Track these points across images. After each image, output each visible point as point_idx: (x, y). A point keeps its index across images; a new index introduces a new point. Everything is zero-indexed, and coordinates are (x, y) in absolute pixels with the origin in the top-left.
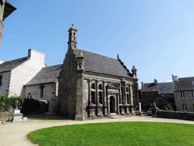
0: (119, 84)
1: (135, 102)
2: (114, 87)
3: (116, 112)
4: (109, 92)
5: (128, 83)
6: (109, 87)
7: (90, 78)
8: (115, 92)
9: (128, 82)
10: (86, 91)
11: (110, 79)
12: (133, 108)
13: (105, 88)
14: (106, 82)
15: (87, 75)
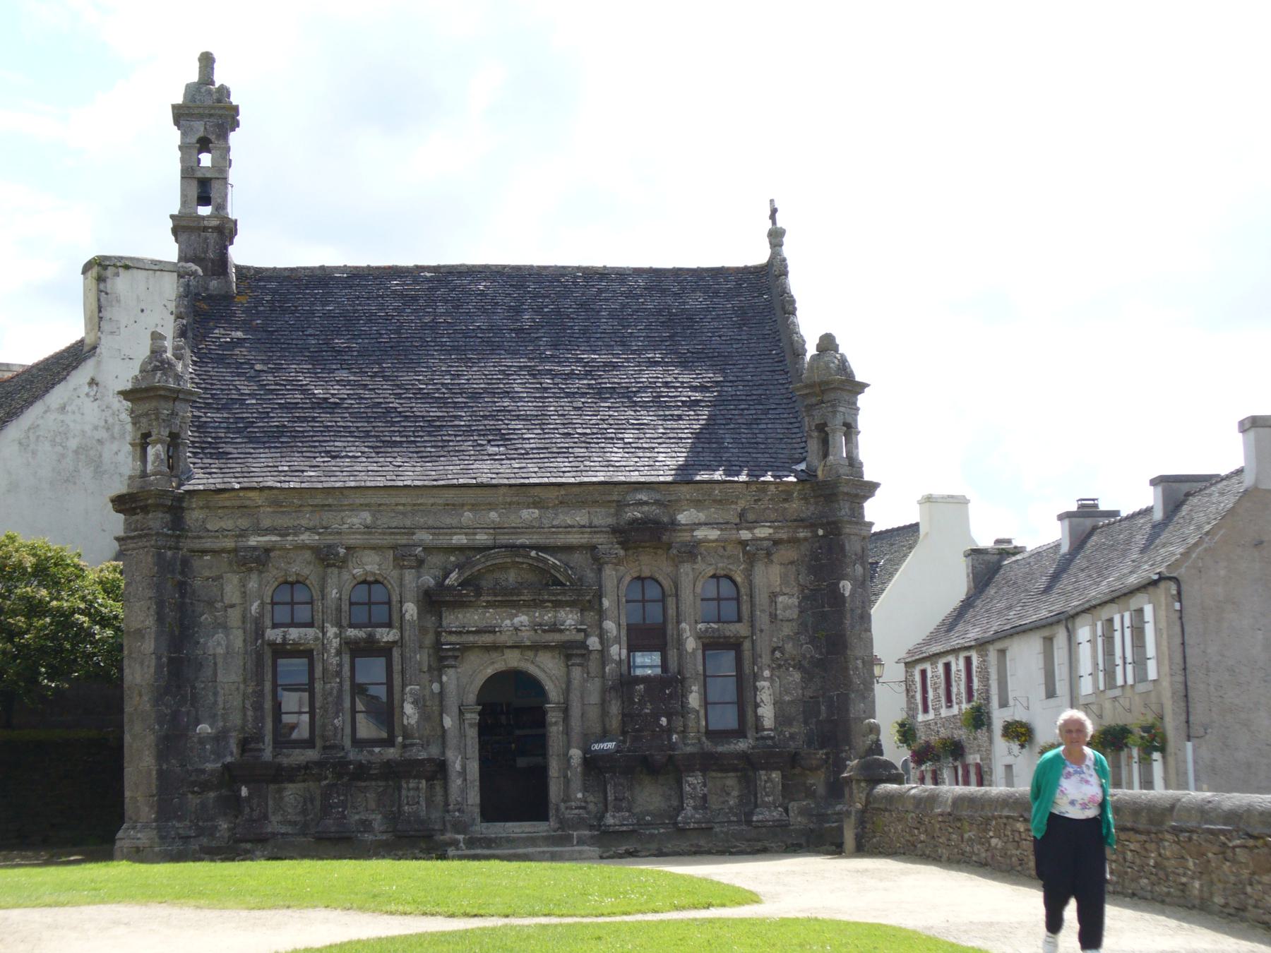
3: (552, 813)
4: (453, 639)
7: (253, 541)
8: (527, 637)
10: (220, 651)
12: (776, 776)
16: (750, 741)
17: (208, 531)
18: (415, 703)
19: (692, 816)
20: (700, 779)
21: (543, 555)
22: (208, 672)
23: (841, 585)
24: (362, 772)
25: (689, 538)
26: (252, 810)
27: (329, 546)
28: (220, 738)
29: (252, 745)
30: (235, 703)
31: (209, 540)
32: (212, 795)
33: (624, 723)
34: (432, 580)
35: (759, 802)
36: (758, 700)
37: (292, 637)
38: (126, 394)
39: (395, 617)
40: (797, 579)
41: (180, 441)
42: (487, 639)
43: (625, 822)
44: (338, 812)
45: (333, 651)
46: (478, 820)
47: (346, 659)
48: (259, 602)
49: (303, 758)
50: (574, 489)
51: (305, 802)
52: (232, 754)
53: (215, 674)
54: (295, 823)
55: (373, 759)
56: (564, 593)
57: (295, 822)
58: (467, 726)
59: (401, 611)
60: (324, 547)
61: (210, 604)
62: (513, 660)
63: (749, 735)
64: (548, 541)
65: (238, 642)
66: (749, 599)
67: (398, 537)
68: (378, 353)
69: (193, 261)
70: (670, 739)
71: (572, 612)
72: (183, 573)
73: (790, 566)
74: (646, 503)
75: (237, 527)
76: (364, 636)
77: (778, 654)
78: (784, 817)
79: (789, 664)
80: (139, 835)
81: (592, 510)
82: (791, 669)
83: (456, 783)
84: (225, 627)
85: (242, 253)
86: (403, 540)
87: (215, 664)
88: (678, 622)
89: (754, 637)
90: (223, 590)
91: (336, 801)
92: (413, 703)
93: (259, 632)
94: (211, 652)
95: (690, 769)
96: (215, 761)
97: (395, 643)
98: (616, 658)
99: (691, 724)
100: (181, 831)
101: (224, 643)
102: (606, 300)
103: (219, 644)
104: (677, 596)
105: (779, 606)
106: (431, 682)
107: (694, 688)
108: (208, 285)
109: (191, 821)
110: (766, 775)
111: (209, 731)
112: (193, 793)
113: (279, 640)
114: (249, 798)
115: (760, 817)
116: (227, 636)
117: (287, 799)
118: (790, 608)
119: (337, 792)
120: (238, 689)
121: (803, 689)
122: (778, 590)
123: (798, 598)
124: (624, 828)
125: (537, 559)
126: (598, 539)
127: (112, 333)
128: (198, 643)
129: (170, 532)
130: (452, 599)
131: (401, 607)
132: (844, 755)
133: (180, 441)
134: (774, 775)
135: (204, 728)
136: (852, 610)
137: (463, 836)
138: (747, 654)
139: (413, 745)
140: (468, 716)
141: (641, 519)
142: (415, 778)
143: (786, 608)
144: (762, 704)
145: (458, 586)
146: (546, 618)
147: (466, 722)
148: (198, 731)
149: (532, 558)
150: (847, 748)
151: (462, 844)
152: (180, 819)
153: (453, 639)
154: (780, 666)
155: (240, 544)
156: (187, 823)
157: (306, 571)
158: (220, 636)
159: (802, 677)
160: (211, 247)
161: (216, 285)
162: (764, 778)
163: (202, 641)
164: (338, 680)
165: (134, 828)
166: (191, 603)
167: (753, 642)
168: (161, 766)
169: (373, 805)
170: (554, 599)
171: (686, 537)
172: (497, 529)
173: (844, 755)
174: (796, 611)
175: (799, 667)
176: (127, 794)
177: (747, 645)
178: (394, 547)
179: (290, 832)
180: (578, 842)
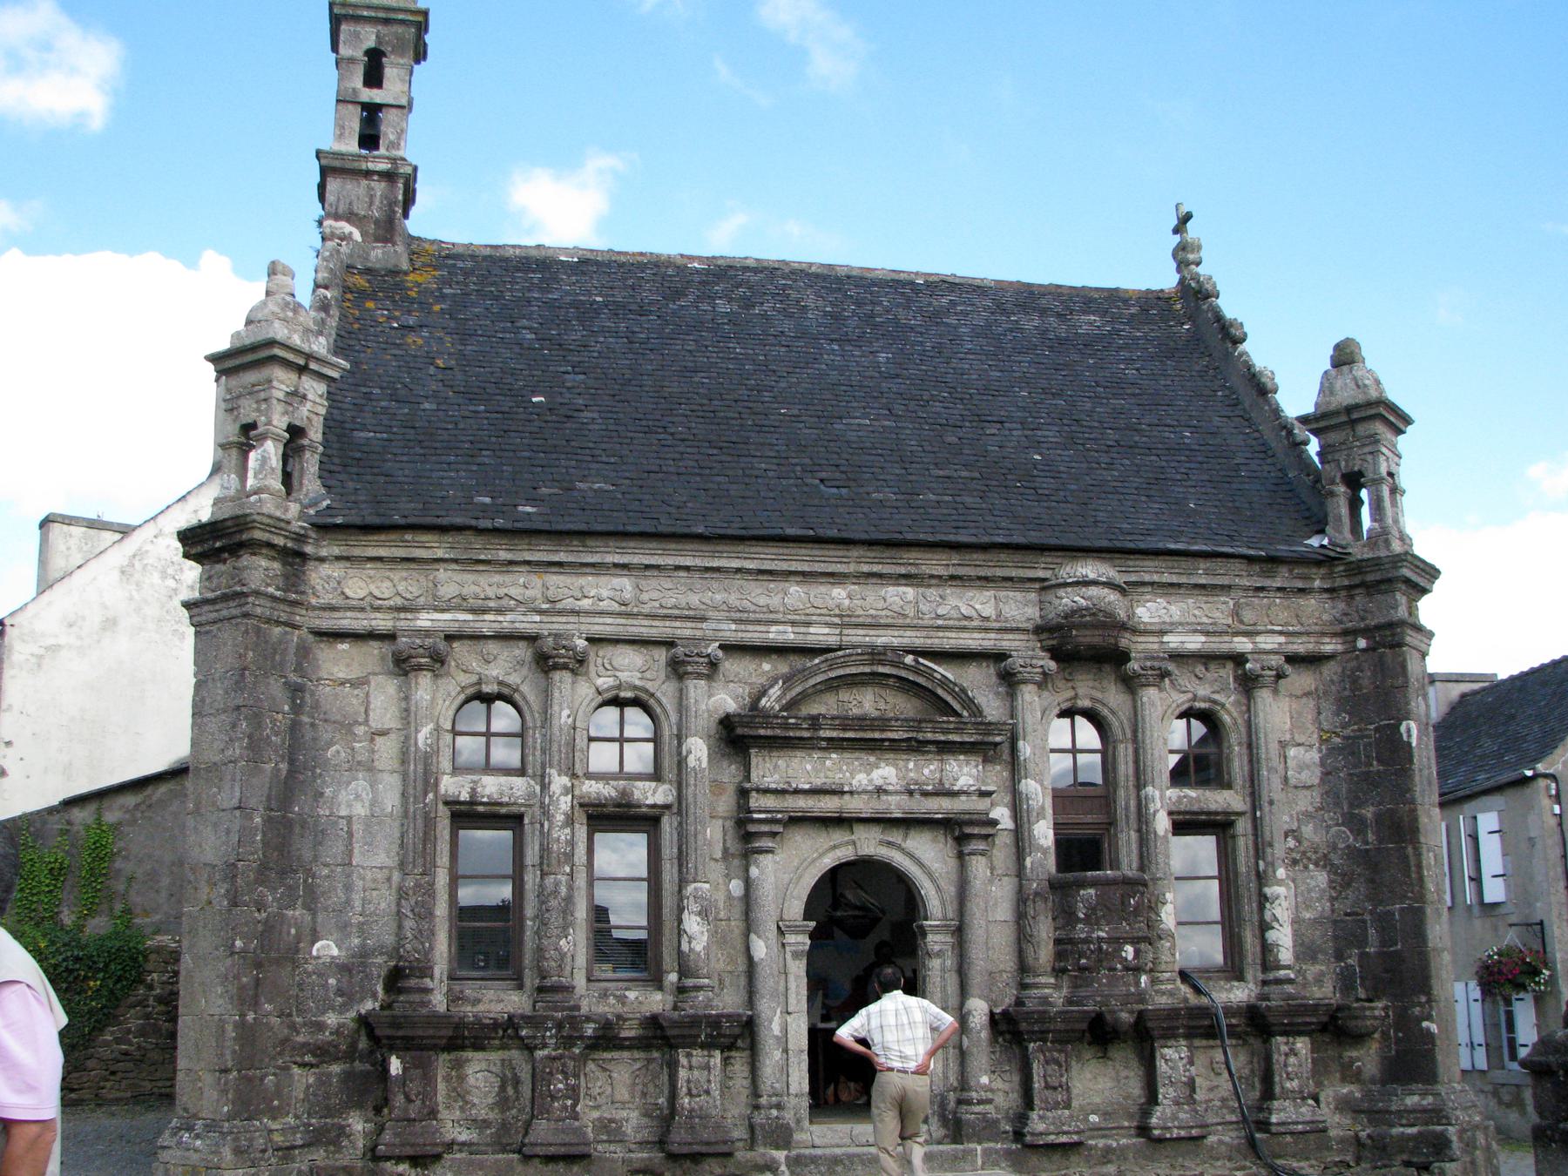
1: (1363, 942)
2: (882, 723)
4: (770, 802)
5: (1195, 643)
6: (766, 717)
7: (425, 620)
8: (895, 805)
9: (1217, 611)
10: (360, 810)
12: (1302, 1044)
14: (712, 648)
16: (1251, 985)
17: (347, 598)
18: (704, 913)
19: (1174, 1117)
20: (1184, 1053)
21: (926, 662)
22: (333, 850)
23: (1403, 728)
24: (607, 1039)
25: (1156, 646)
26: (409, 1100)
29: (413, 982)
30: (383, 905)
31: (349, 614)
32: (336, 1068)
33: (1060, 955)
34: (730, 701)
35: (1277, 1089)
36: (1268, 916)
37: (487, 791)
39: (668, 762)
40: (1317, 721)
41: (305, 442)
42: (828, 805)
43: (1065, 1128)
44: (565, 1108)
45: (560, 818)
46: (806, 1123)
47: (582, 832)
48: (431, 726)
49: (499, 1007)
51: (503, 1088)
52: (374, 996)
53: (350, 853)
54: (486, 1124)
56: (957, 730)
57: (484, 1121)
58: (789, 956)
59: (680, 754)
60: (550, 635)
61: (346, 727)
62: (869, 843)
63: (1249, 975)
64: (929, 641)
65: (391, 800)
66: (1245, 751)
67: (678, 624)
68: (630, 356)
69: (348, 221)
71: (968, 763)
72: (299, 669)
73: (1304, 700)
74: (1094, 583)
75: (398, 594)
76: (614, 794)
79: (1309, 859)
80: (198, 1142)
81: (1002, 594)
82: (1311, 866)
83: (771, 1058)
84: (370, 768)
85: (424, 222)
86: (684, 630)
87: (350, 834)
88: (1140, 784)
89: (1258, 814)
90: (368, 703)
91: (560, 1086)
92: (699, 914)
93: (429, 781)
94: (343, 813)
95: (1170, 1035)
96: (343, 1008)
97: (667, 807)
100: (277, 1138)
101: (367, 796)
102: (965, 313)
103: (358, 797)
104: (1135, 740)
106: (728, 877)
108: (368, 254)
109: (297, 1117)
110: (1287, 1043)
111: (335, 952)
112: (303, 1065)
113: (464, 796)
115: (1282, 1116)
116: (373, 785)
117: (471, 1080)
118: (1308, 767)
119: (563, 1072)
120: (389, 879)
121: (1332, 899)
122: (1288, 737)
123: (1320, 751)
124: (1064, 1139)
125: (915, 669)
126: (1007, 642)
128: (322, 794)
129: (278, 593)
130: (769, 732)
131: (680, 745)
132: (1417, 1010)
133: (305, 442)
134: (1299, 1045)
136: (1421, 770)
137: (785, 1152)
138: (1243, 844)
139: (698, 988)
140: (791, 938)
141: (1087, 609)
142: (703, 1046)
143: (1302, 767)
144: (1275, 925)
145: (780, 710)
146: (926, 771)
147: (788, 948)
148: (314, 953)
149: (906, 667)
150: (1423, 999)
151: (783, 1168)
152: (275, 1114)
153: (770, 802)
154: (1295, 862)
155: (402, 624)
156: (291, 1120)
157: (514, 679)
158: (361, 784)
159: (1331, 881)
160: (377, 202)
161: (380, 256)
162: (1284, 1048)
163: (328, 791)
164: (568, 869)
165: (190, 1129)
166: (313, 725)
167: (1256, 824)
168: (243, 1015)
169: (623, 1093)
170: (942, 738)
171: (1149, 644)
172: (845, 620)
173: (1417, 1010)
174: (1318, 771)
175: (1324, 862)
176: (182, 1063)
177: (1243, 826)
178: (669, 644)
179: (475, 1141)
180: (983, 1163)
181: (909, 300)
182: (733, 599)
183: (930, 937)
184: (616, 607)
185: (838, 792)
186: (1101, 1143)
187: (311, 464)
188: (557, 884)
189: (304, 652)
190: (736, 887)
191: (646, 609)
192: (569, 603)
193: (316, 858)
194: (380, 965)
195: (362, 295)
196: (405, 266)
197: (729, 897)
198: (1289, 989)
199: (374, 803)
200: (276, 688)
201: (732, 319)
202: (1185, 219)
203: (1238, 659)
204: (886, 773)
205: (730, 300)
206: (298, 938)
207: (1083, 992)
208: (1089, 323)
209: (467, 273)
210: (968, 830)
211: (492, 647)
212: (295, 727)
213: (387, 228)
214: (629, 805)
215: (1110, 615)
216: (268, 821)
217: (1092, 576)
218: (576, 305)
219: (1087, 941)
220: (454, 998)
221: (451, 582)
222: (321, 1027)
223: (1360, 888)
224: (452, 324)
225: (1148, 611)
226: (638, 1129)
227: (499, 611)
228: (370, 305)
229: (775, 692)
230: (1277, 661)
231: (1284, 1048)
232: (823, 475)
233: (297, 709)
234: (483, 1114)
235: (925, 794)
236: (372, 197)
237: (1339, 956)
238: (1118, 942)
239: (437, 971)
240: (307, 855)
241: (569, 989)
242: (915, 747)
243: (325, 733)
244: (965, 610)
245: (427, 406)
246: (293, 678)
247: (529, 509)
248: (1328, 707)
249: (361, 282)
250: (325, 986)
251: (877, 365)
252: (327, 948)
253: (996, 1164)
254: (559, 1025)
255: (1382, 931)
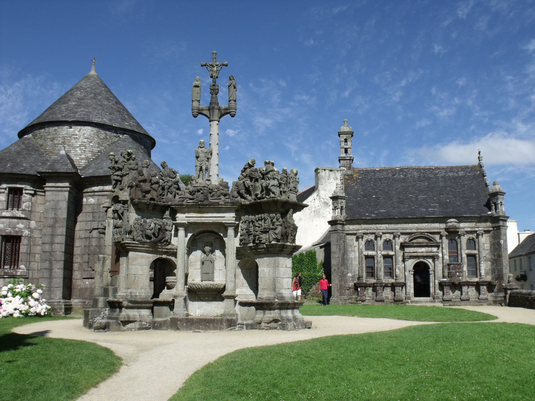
0: (439, 233)
1: (495, 272)
2: (423, 243)
3: (431, 295)
5: (469, 229)
7: (360, 231)
8: (425, 254)
9: (473, 224)
10: (353, 257)
11: (410, 225)
12: (485, 287)
13: (398, 247)
14: (399, 234)
15: (351, 227)
18: (399, 269)
19: (465, 297)
20: (467, 288)
22: (350, 262)
24: (386, 286)
27: (378, 233)
28: (353, 277)
32: (352, 290)
33: (449, 274)
35: (481, 293)
38: (331, 198)
42: (415, 254)
45: (379, 257)
46: (413, 297)
47: (382, 259)
50: (436, 219)
53: (352, 262)
54: (371, 297)
55: (389, 282)
61: (351, 246)
62: (422, 260)
65: (357, 255)
70: (459, 278)
72: (344, 239)
77: (485, 258)
78: (487, 297)
83: (408, 288)
84: (354, 251)
86: (395, 231)
93: (362, 253)
95: (464, 285)
96: (352, 282)
97: (394, 255)
98: (446, 259)
99: (464, 275)
100: (345, 298)
101: (354, 255)
102: (441, 174)
105: (485, 246)
107: (465, 266)
113: (367, 254)
114: (360, 291)
116: (355, 253)
121: (491, 266)
124: (448, 299)
125: (427, 235)
126: (440, 230)
127: (322, 184)
135: (350, 275)
138: (477, 259)
139: (398, 279)
140: (411, 272)
143: (487, 247)
149: (426, 235)
154: (485, 261)
158: (353, 253)
162: (482, 287)
163: (349, 254)
165: (334, 297)
167: (479, 255)
171: (462, 230)
173: (502, 282)
175: (490, 261)
181: (432, 172)
182: (402, 226)
183: (430, 272)
184: (386, 228)
185: (417, 253)
186: (454, 300)
187: (344, 211)
188: (379, 266)
189: (345, 236)
190: (403, 265)
191: (389, 228)
192: (379, 228)
193: (348, 263)
194: (357, 276)
195: (348, 180)
196: (353, 174)
197: (402, 267)
198: (483, 279)
199: (355, 256)
200: (342, 242)
201: (403, 178)
202: (479, 153)
203: (476, 231)
204: (423, 249)
205: (403, 175)
206: (346, 274)
207: (451, 279)
208: (461, 174)
209: (362, 174)
210: (435, 257)
211: (369, 235)
212: (344, 247)
213: (350, 168)
214: (389, 255)
215: (456, 226)
216: (342, 259)
217: (453, 221)
218: (379, 178)
219: (452, 272)
220: (366, 281)
221: (364, 226)
222: (349, 285)
223: (495, 264)
224: (361, 184)
225: (462, 225)
226: (391, 298)
227: (370, 230)
228: (349, 181)
229: (407, 239)
230: (482, 231)
231: (482, 287)
232: (415, 206)
233: (344, 244)
234: (370, 296)
235: (429, 252)
236: (347, 163)
237: (492, 275)
238: (456, 272)
239: (364, 277)
240: (347, 263)
241: (381, 279)
242: (427, 246)
243: (348, 247)
244: (435, 226)
245: (358, 199)
246: (344, 240)
247: (373, 215)
248: (491, 238)
249: (347, 177)
250: (350, 279)
251: (425, 185)
252: (350, 275)
253: (439, 302)
254: (380, 284)
255: (497, 271)
